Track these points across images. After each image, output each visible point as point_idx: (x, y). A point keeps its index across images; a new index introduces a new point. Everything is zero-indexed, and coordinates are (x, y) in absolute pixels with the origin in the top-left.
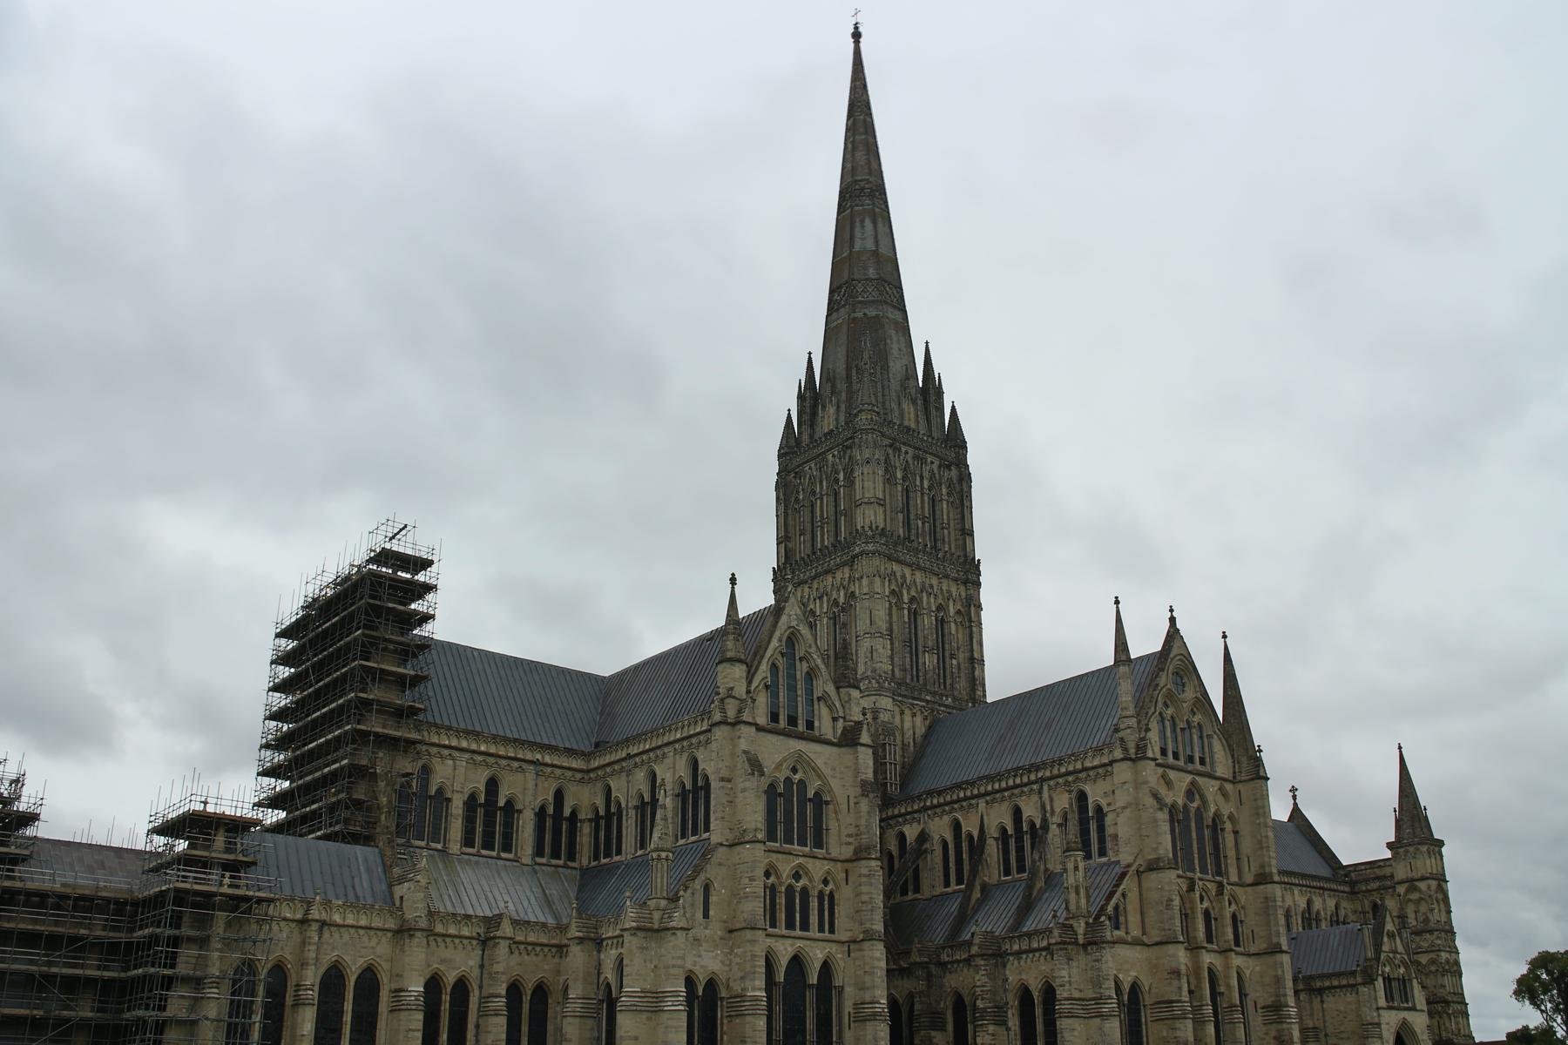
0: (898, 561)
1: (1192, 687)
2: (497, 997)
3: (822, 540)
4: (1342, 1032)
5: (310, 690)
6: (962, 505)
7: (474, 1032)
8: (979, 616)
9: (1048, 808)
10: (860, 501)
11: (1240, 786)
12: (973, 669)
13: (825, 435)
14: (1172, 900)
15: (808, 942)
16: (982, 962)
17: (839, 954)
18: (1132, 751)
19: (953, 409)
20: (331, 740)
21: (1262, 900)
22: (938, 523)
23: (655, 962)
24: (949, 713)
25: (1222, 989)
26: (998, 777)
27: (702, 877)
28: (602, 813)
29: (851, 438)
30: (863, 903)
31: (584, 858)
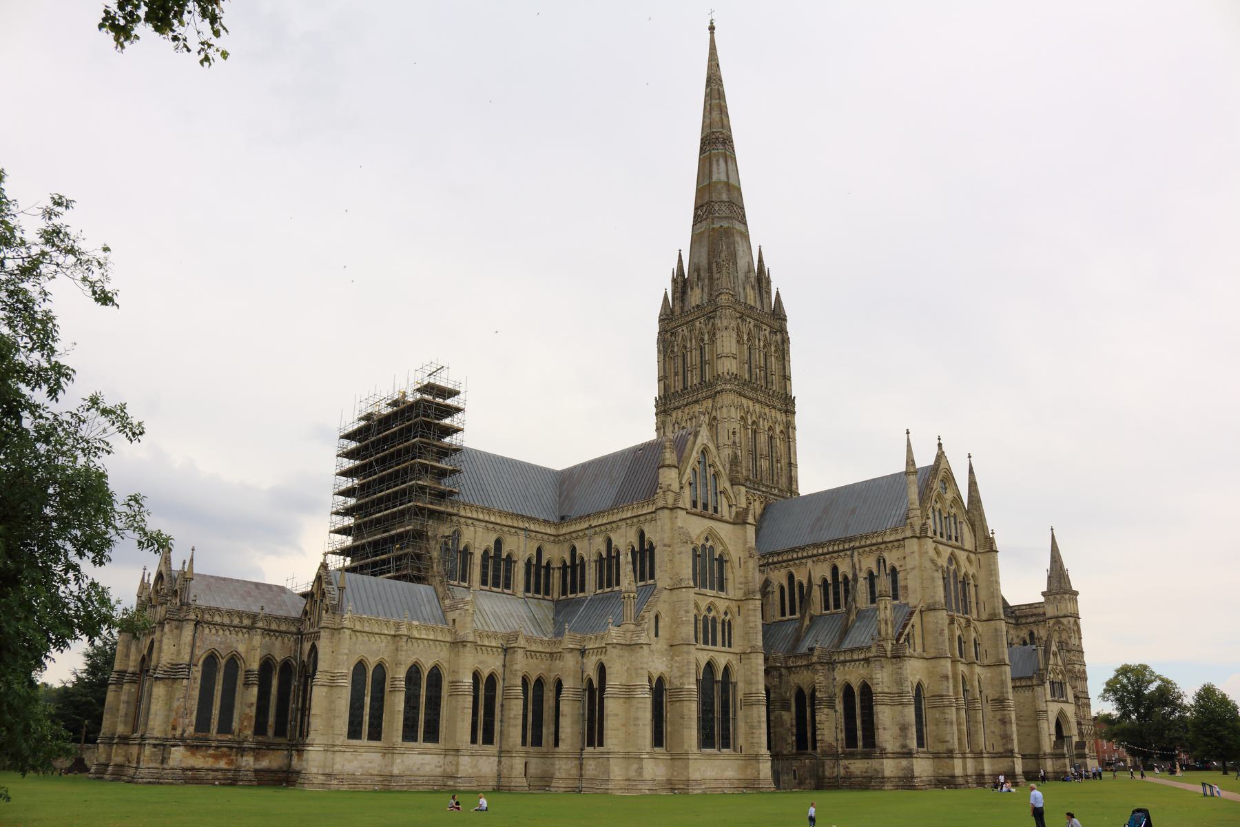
0: (745, 397)
1: (952, 491)
2: (516, 686)
4: (1021, 716)
5: (375, 477)
6: (784, 358)
7: (500, 708)
8: (794, 435)
9: (857, 567)
10: (721, 355)
11: (979, 556)
12: (791, 470)
13: (693, 308)
14: (943, 630)
15: (716, 653)
16: (820, 668)
17: (734, 661)
18: (918, 532)
19: (778, 293)
20: (395, 512)
21: (994, 631)
23: (628, 665)
24: (776, 500)
25: (968, 688)
26: (822, 545)
28: (568, 563)
30: (750, 628)
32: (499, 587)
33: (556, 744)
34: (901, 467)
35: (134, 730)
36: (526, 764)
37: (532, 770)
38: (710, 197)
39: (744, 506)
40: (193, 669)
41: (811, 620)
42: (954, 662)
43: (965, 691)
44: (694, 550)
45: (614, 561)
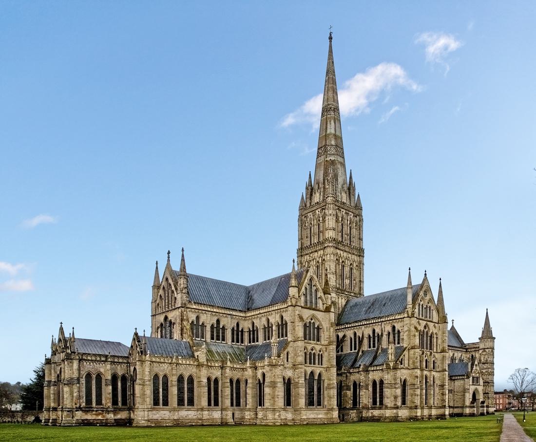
0: (339, 249)
3: (314, 240)
6: (360, 229)
9: (383, 330)
13: (316, 203)
22: (352, 236)
27: (286, 350)
28: (251, 330)
29: (325, 206)
31: (246, 343)
32: (219, 340)
34: (405, 285)
35: (59, 405)
36: (233, 414)
37: (236, 416)
38: (326, 142)
39: (330, 304)
40: (81, 380)
41: (362, 352)
42: (422, 370)
43: (426, 382)
44: (305, 325)
45: (271, 329)
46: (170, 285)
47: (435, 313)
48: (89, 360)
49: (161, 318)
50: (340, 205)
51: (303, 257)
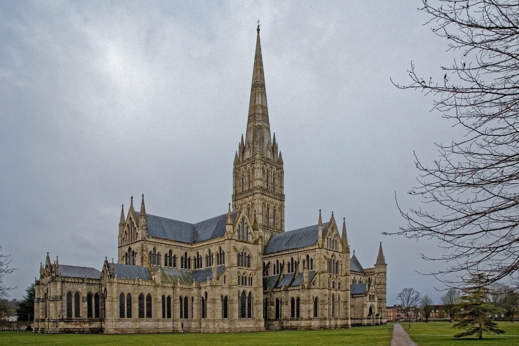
6: (281, 180)
9: (300, 258)
13: (247, 159)
19: (280, 153)
22: (275, 185)
28: (196, 258)
29: (254, 161)
31: (192, 268)
32: (171, 266)
33: (192, 318)
34: (317, 223)
35: (46, 317)
36: (182, 324)
37: (185, 326)
38: (255, 111)
39: (258, 238)
40: (63, 297)
41: (283, 276)
42: (330, 290)
43: (333, 299)
45: (212, 257)
46: (133, 223)
47: (340, 246)
48: (69, 282)
49: (126, 249)
50: (266, 161)
51: (237, 201)
